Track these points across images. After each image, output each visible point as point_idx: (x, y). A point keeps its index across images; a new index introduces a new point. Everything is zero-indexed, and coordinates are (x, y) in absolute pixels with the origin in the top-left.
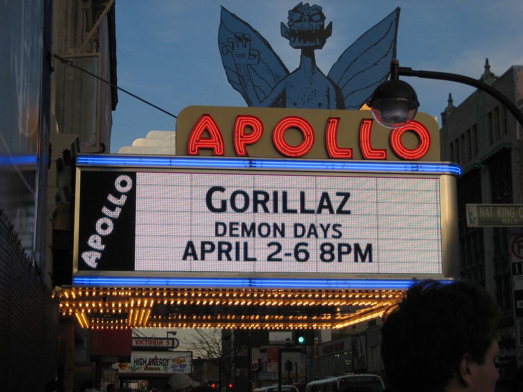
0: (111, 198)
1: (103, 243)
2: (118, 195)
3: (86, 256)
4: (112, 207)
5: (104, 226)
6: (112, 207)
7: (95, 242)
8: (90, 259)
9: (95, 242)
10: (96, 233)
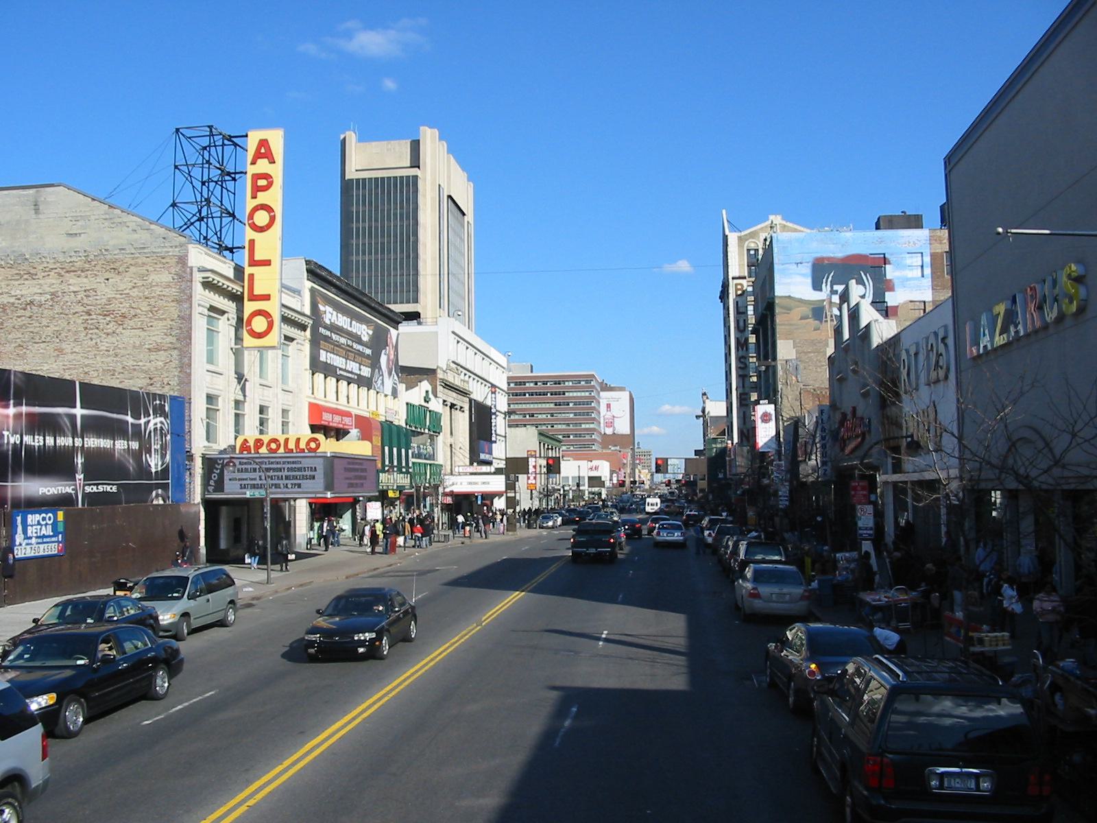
0: (217, 466)
2: (219, 464)
3: (209, 488)
6: (217, 469)
7: (212, 483)
8: (211, 489)
9: (212, 483)
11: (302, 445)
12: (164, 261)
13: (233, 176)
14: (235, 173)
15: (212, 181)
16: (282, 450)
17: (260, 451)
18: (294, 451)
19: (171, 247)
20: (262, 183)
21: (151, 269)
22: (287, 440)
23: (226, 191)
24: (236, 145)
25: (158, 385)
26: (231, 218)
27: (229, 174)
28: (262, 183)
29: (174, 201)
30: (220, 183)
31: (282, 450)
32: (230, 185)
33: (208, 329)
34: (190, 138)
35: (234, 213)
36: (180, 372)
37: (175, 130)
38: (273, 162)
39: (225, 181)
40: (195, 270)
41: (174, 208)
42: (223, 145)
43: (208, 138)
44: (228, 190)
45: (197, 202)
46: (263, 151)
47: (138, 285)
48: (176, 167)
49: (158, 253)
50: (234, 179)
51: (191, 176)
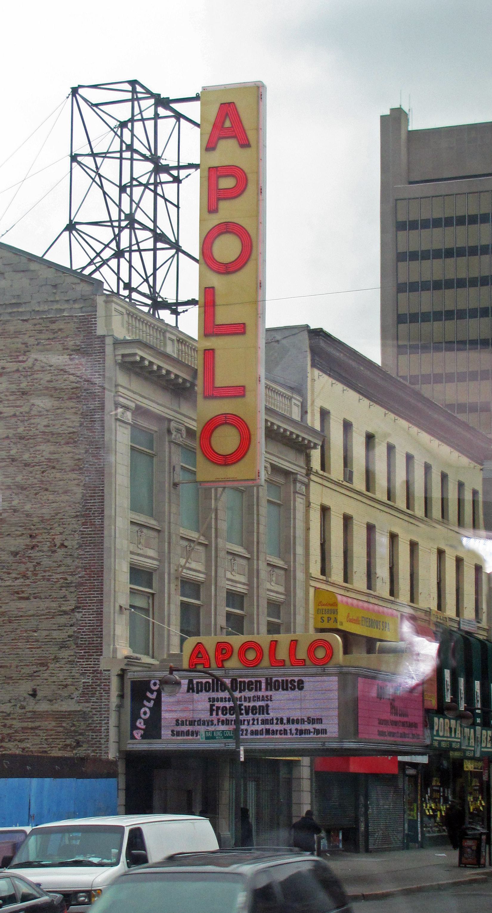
0: (149, 694)
1: (144, 725)
2: (152, 692)
3: (135, 732)
4: (149, 700)
5: (145, 713)
6: (149, 700)
7: (140, 724)
9: (140, 724)
10: (141, 718)
11: (302, 653)
12: (54, 326)
13: (175, 173)
14: (179, 168)
15: (141, 184)
16: (266, 662)
17: (228, 664)
18: (288, 663)
19: (67, 301)
20: (227, 183)
21: (31, 341)
22: (274, 645)
23: (163, 200)
24: (178, 116)
25: (45, 549)
26: (173, 251)
27: (167, 169)
28: (227, 183)
29: (71, 221)
30: (152, 187)
31: (266, 662)
32: (170, 191)
33: (133, 449)
34: (97, 105)
35: (177, 241)
36: (83, 524)
37: (71, 90)
38: (245, 144)
39: (161, 183)
40: (109, 341)
41: (71, 232)
42: (157, 117)
43: (130, 103)
44: (166, 200)
45: (111, 221)
46: (228, 124)
47: (8, 370)
48: (74, 158)
49: (44, 312)
50: (177, 180)
51: (100, 176)
